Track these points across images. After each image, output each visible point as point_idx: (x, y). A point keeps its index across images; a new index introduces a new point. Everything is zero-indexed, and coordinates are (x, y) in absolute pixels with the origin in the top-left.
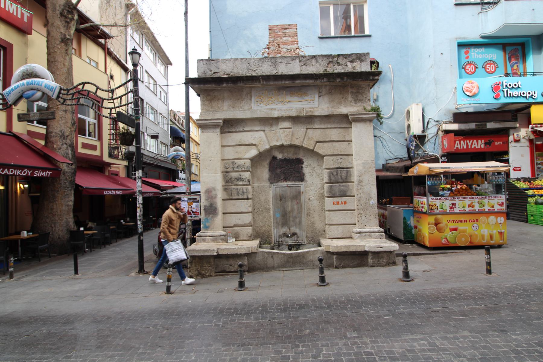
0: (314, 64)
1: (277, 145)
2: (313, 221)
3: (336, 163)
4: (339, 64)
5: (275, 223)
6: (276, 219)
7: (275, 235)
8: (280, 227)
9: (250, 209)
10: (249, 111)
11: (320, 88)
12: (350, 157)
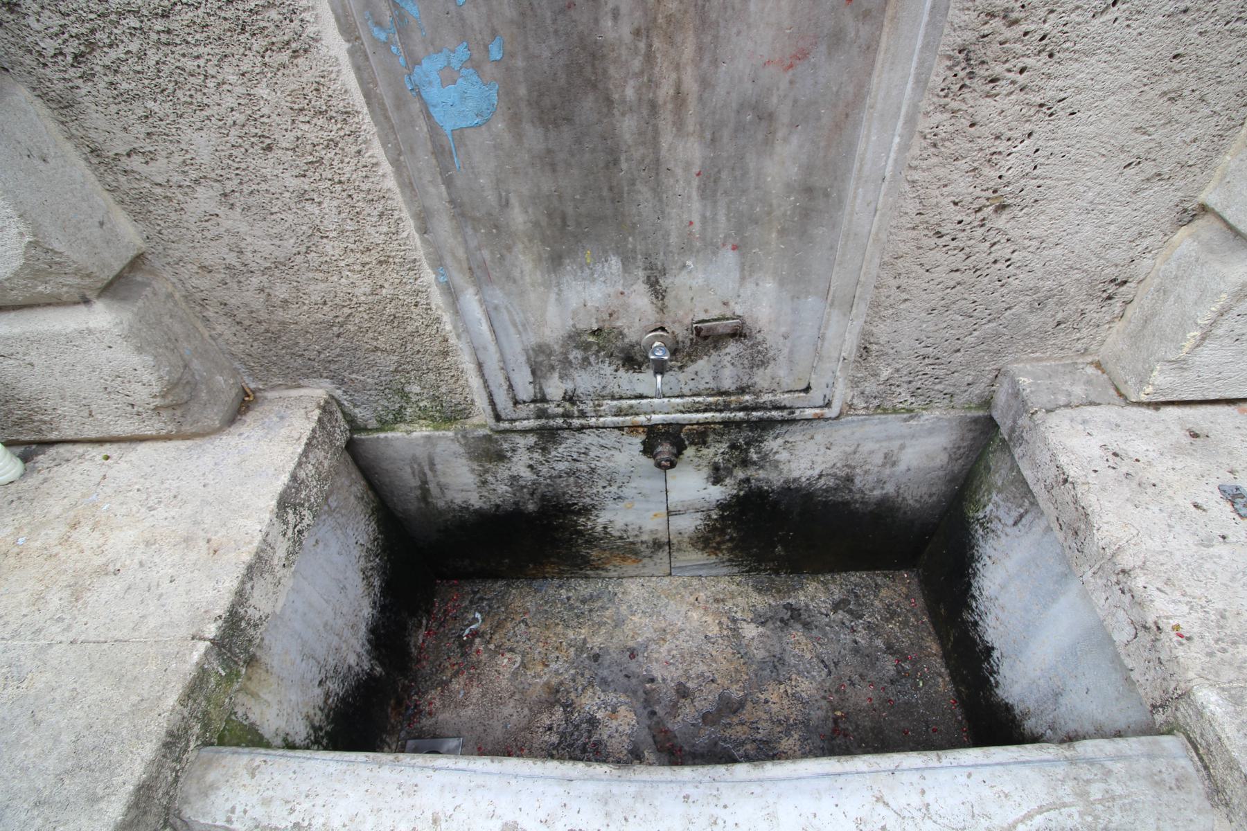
2: (1014, 164)
5: (444, 226)
6: (440, 152)
7: (475, 351)
8: (524, 262)
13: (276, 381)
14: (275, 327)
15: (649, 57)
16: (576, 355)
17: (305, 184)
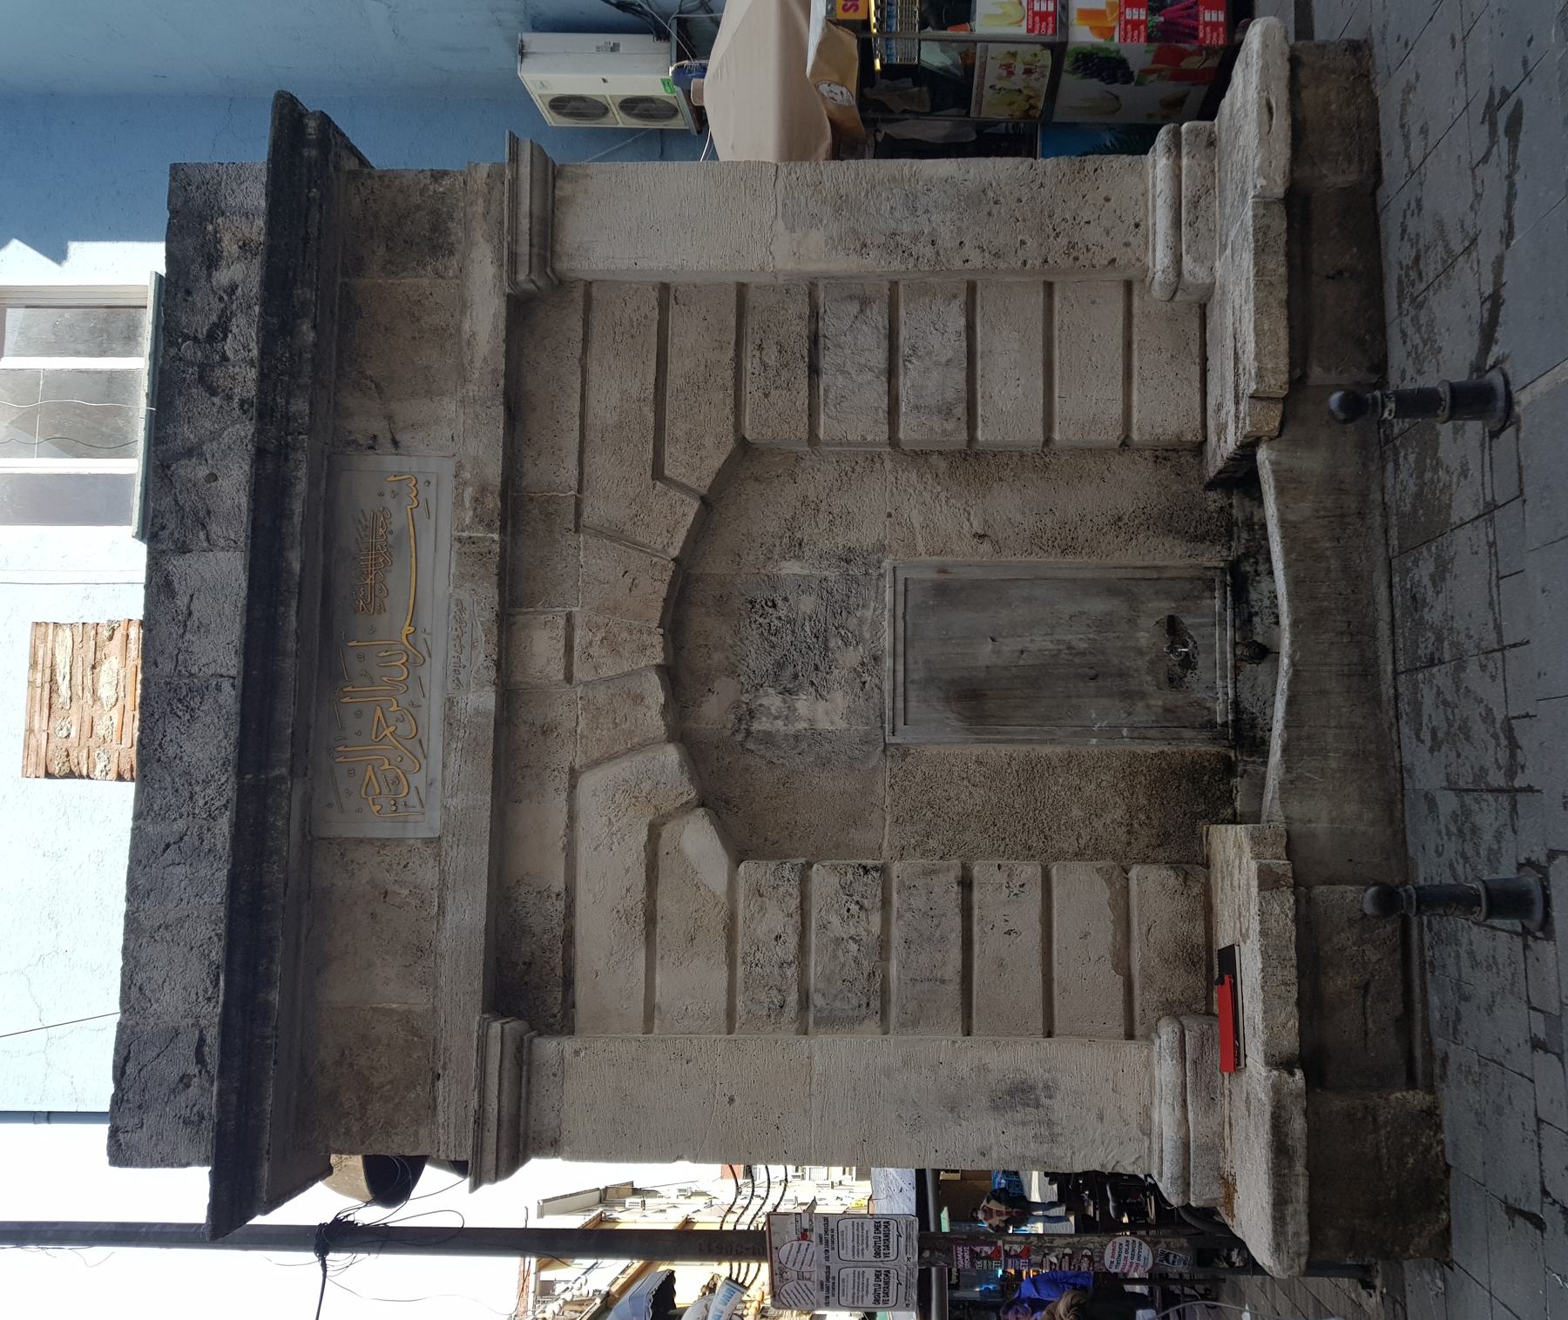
0: (202, 472)
1: (662, 700)
3: (784, 373)
4: (219, 330)
9: (1029, 871)
10: (453, 853)
11: (349, 443)
12: (752, 297)
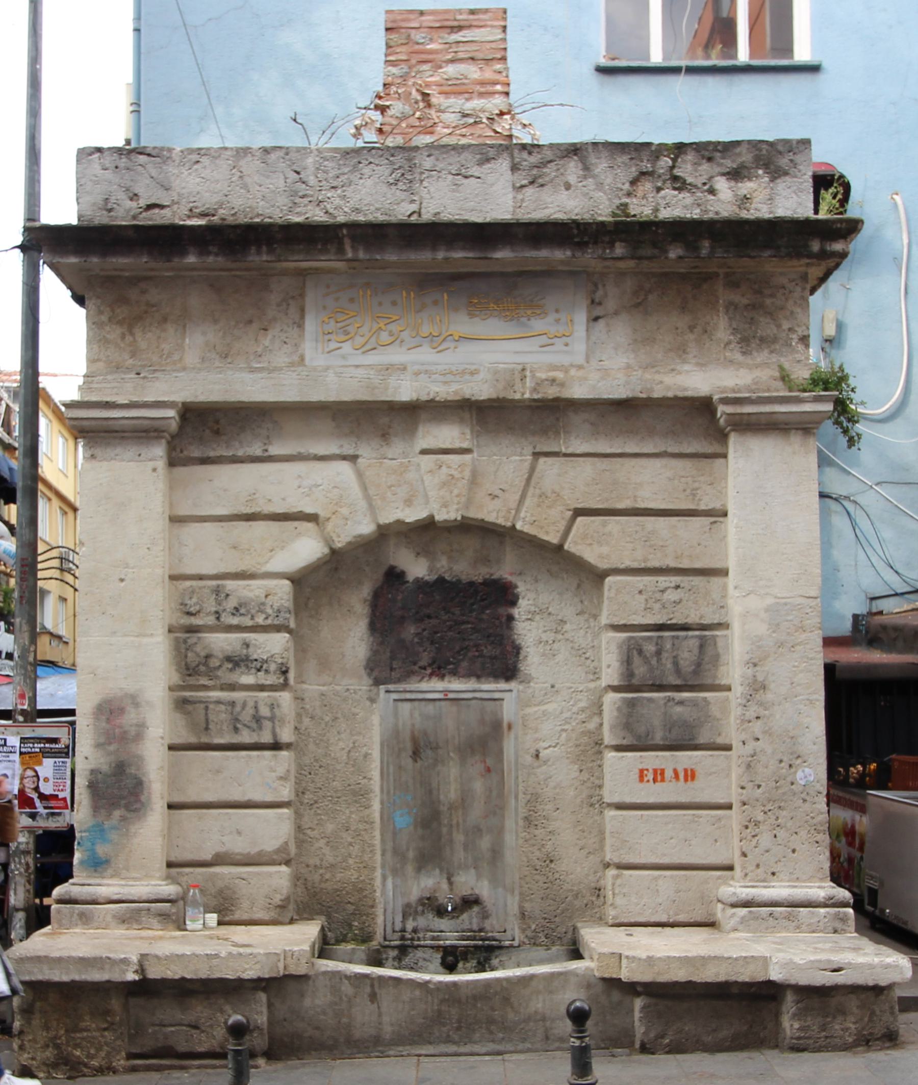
0: (572, 179)
1: (407, 521)
2: (549, 847)
3: (657, 606)
4: (679, 184)
5: (389, 855)
6: (395, 834)
7: (385, 903)
8: (410, 869)
9: (286, 792)
10: (294, 375)
11: (596, 285)
12: (716, 581)
13: (305, 916)
14: (318, 890)
15: (451, 814)
16: (420, 908)
17: (353, 840)
